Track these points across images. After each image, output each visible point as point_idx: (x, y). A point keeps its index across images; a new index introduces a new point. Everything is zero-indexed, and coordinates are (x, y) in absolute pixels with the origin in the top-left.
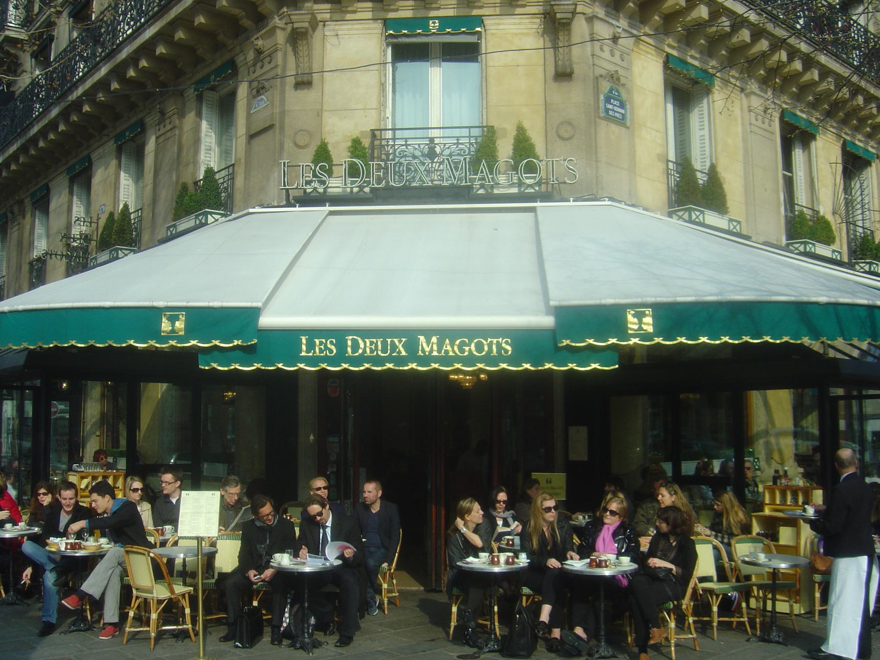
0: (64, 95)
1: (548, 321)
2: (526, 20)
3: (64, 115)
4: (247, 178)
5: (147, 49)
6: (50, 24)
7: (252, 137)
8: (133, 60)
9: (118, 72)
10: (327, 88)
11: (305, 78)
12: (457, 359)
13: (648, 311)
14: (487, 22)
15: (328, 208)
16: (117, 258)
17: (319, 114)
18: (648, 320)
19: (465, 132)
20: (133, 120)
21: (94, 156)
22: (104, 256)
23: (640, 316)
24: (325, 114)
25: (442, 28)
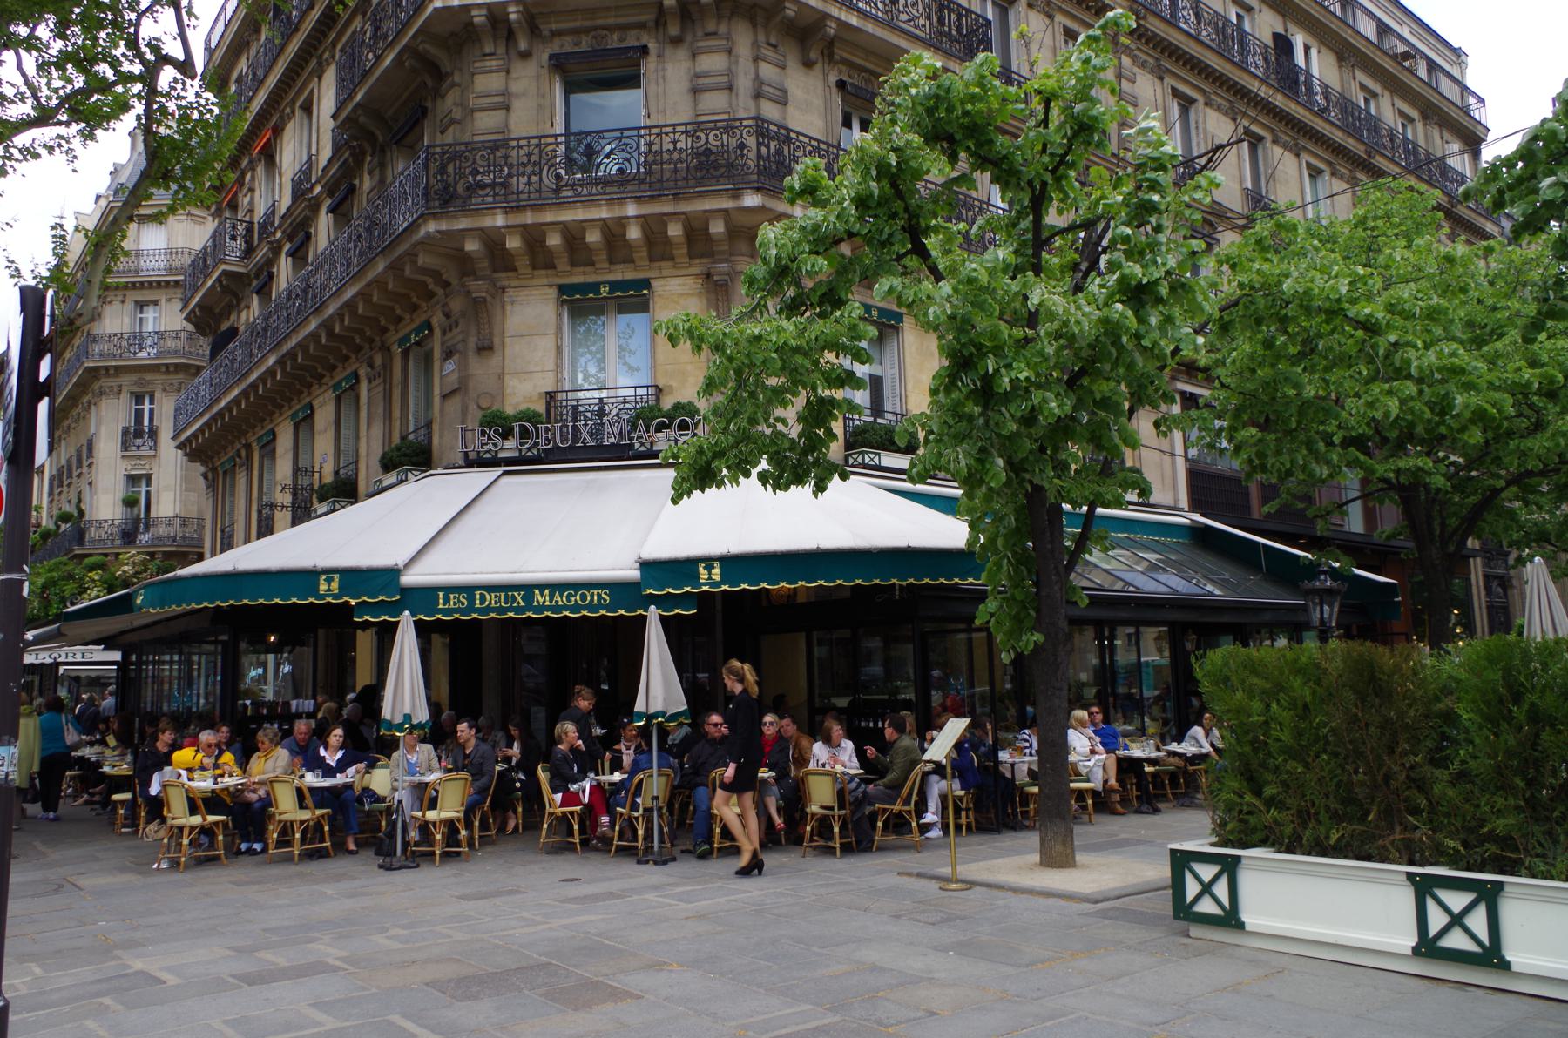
0: (279, 344)
1: (634, 574)
2: (690, 281)
3: (281, 362)
4: (441, 437)
5: (350, 305)
6: (270, 262)
7: (445, 397)
8: (339, 315)
9: (327, 325)
10: (507, 351)
11: (486, 343)
12: (565, 608)
13: (717, 564)
14: (655, 283)
15: (501, 469)
16: (334, 511)
17: (501, 377)
18: (716, 571)
19: (631, 392)
20: (348, 372)
21: (316, 404)
22: (322, 508)
23: (709, 568)
24: (507, 378)
25: (612, 291)
